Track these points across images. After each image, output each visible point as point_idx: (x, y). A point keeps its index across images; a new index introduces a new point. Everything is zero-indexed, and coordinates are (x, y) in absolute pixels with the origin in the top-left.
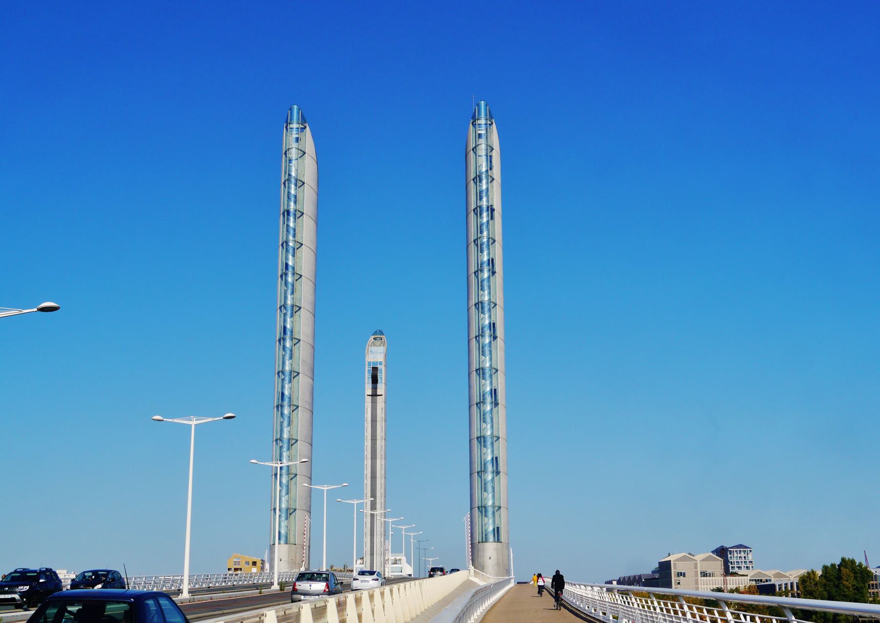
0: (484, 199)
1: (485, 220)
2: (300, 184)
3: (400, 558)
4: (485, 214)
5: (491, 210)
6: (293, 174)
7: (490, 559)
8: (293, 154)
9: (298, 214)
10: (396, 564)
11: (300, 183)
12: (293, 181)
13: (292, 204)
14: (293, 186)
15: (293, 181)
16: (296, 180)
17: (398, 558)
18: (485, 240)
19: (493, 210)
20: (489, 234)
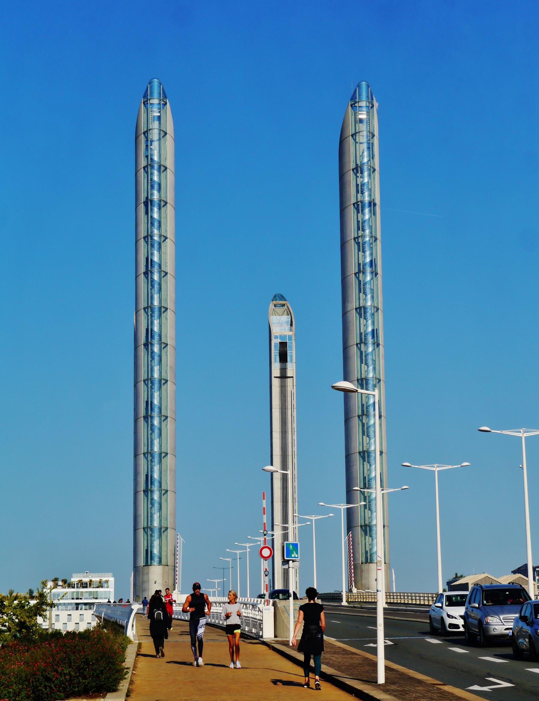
0: (366, 194)
1: (367, 217)
2: (162, 169)
3: (107, 579)
4: (367, 210)
5: (372, 204)
6: (156, 158)
8: (155, 135)
10: (102, 587)
11: (163, 169)
12: (156, 166)
13: (156, 192)
14: (156, 173)
15: (156, 166)
16: (160, 167)
17: (104, 579)
18: (367, 239)
19: (375, 205)
20: (371, 233)
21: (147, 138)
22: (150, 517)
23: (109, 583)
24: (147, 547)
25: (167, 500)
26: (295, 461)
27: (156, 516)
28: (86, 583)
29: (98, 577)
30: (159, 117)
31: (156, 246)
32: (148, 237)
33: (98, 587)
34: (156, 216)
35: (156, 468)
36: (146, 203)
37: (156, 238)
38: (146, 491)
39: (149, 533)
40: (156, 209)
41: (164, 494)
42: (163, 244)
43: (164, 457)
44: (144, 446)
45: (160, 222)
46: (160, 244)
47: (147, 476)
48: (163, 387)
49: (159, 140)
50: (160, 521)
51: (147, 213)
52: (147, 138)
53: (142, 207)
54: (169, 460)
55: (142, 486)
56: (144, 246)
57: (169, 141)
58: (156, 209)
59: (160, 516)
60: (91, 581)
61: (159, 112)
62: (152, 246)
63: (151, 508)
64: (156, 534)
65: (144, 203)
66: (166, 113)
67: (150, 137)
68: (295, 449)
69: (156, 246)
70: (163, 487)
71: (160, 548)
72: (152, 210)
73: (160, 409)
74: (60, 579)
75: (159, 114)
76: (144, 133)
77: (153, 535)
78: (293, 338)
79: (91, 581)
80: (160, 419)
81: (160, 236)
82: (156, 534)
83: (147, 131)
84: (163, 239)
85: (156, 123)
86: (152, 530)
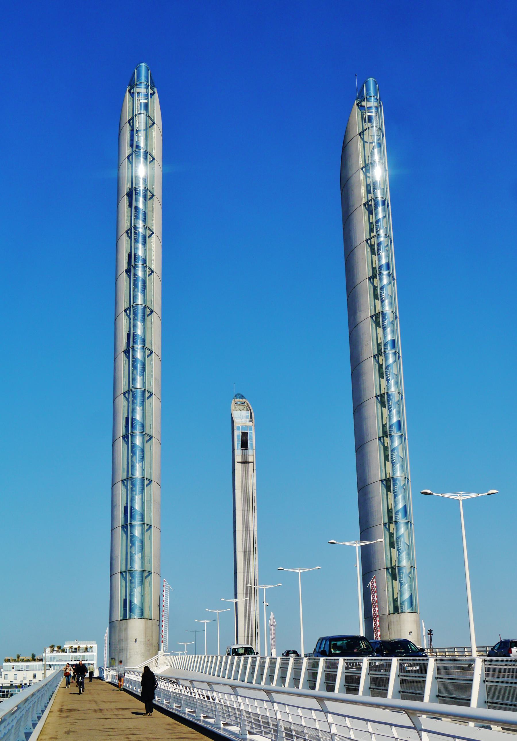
6: (142, 145)
7: (136, 641)
8: (141, 121)
9: (149, 195)
21: (132, 127)
22: (129, 559)
23: (93, 648)
24: (126, 596)
25: (150, 539)
26: (256, 535)
27: (137, 557)
28: (76, 649)
29: (85, 644)
30: (146, 106)
31: (141, 239)
32: (132, 231)
33: (84, 652)
34: (141, 205)
35: (138, 498)
36: (129, 195)
37: (141, 230)
38: (124, 527)
39: (129, 578)
40: (141, 199)
41: (147, 531)
42: (148, 240)
43: (147, 485)
44: (123, 471)
45: (145, 214)
46: (144, 237)
47: (126, 508)
48: (147, 402)
49: (146, 129)
50: (142, 562)
51: (130, 205)
52: (132, 127)
53: (125, 201)
54: (153, 490)
55: (120, 520)
56: (127, 240)
57: (157, 132)
58: (141, 199)
59: (142, 558)
60: (79, 647)
61: (146, 99)
62: (136, 241)
63: (131, 547)
64: (137, 580)
65: (127, 194)
66: (154, 102)
67: (136, 124)
68: (256, 525)
69: (141, 239)
70: (146, 521)
71: (142, 596)
72: (136, 200)
73: (142, 516)
74: (56, 646)
75: (146, 101)
76: (129, 122)
77: (133, 581)
78: (253, 428)
79: (79, 647)
80: (143, 529)
81: (146, 228)
82: (137, 580)
83: (132, 118)
84: (148, 232)
85: (143, 111)
86: (131, 575)
